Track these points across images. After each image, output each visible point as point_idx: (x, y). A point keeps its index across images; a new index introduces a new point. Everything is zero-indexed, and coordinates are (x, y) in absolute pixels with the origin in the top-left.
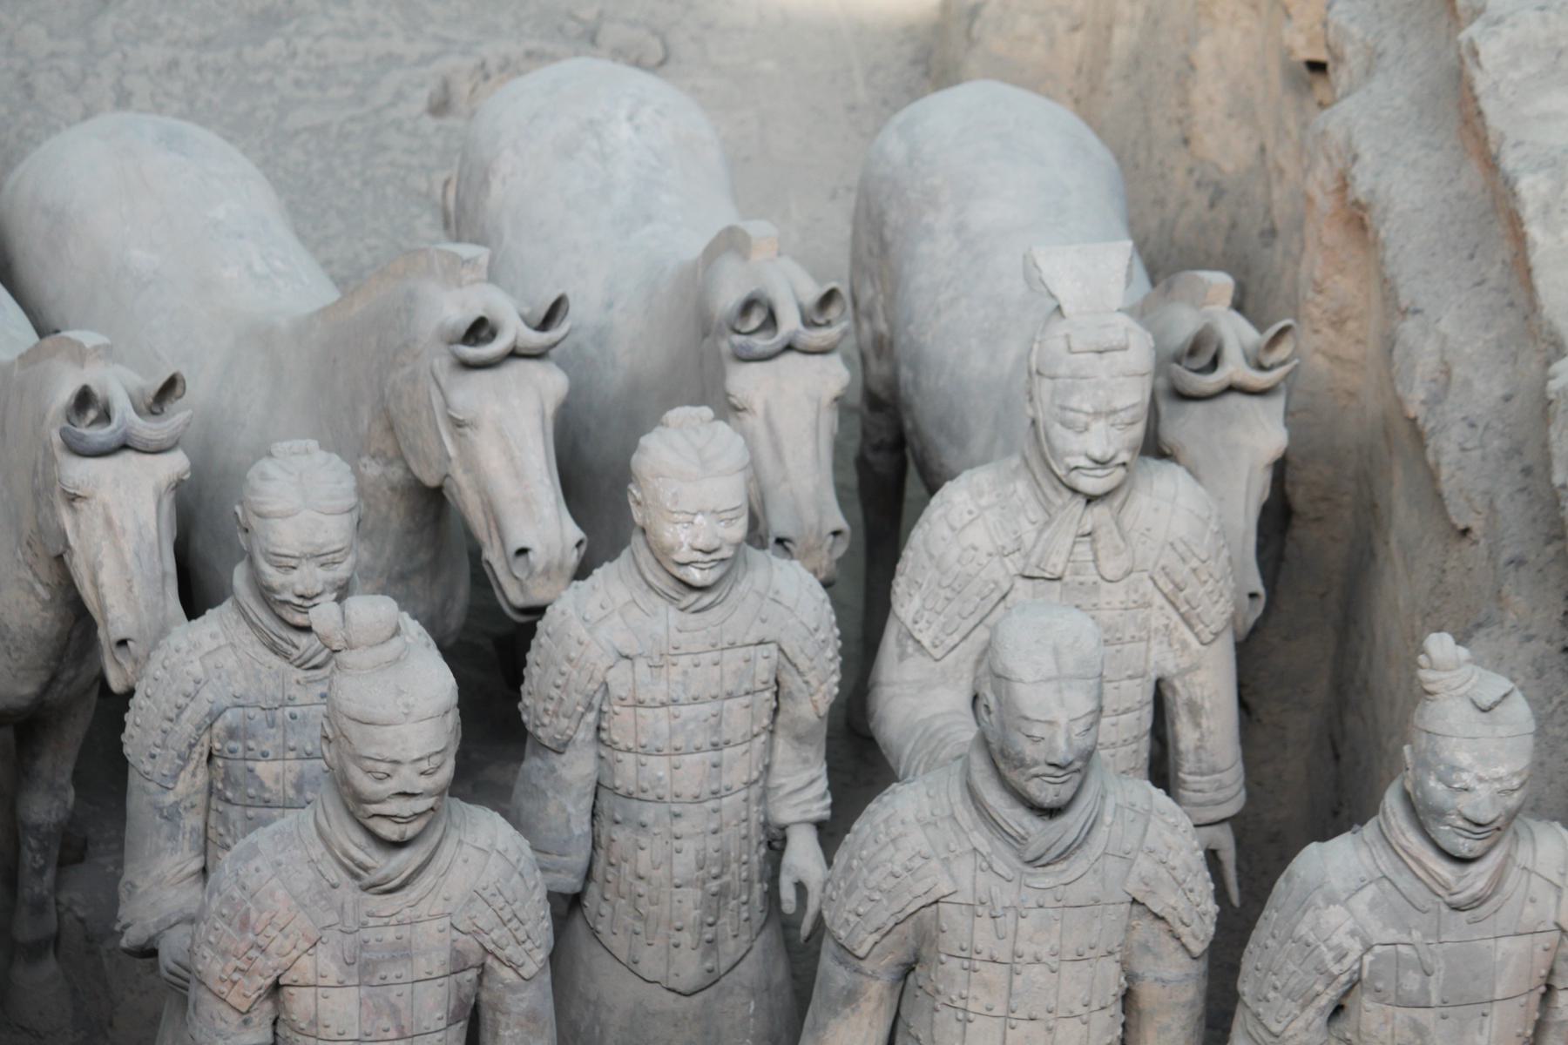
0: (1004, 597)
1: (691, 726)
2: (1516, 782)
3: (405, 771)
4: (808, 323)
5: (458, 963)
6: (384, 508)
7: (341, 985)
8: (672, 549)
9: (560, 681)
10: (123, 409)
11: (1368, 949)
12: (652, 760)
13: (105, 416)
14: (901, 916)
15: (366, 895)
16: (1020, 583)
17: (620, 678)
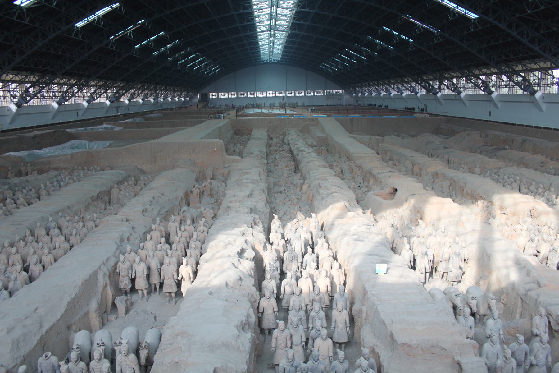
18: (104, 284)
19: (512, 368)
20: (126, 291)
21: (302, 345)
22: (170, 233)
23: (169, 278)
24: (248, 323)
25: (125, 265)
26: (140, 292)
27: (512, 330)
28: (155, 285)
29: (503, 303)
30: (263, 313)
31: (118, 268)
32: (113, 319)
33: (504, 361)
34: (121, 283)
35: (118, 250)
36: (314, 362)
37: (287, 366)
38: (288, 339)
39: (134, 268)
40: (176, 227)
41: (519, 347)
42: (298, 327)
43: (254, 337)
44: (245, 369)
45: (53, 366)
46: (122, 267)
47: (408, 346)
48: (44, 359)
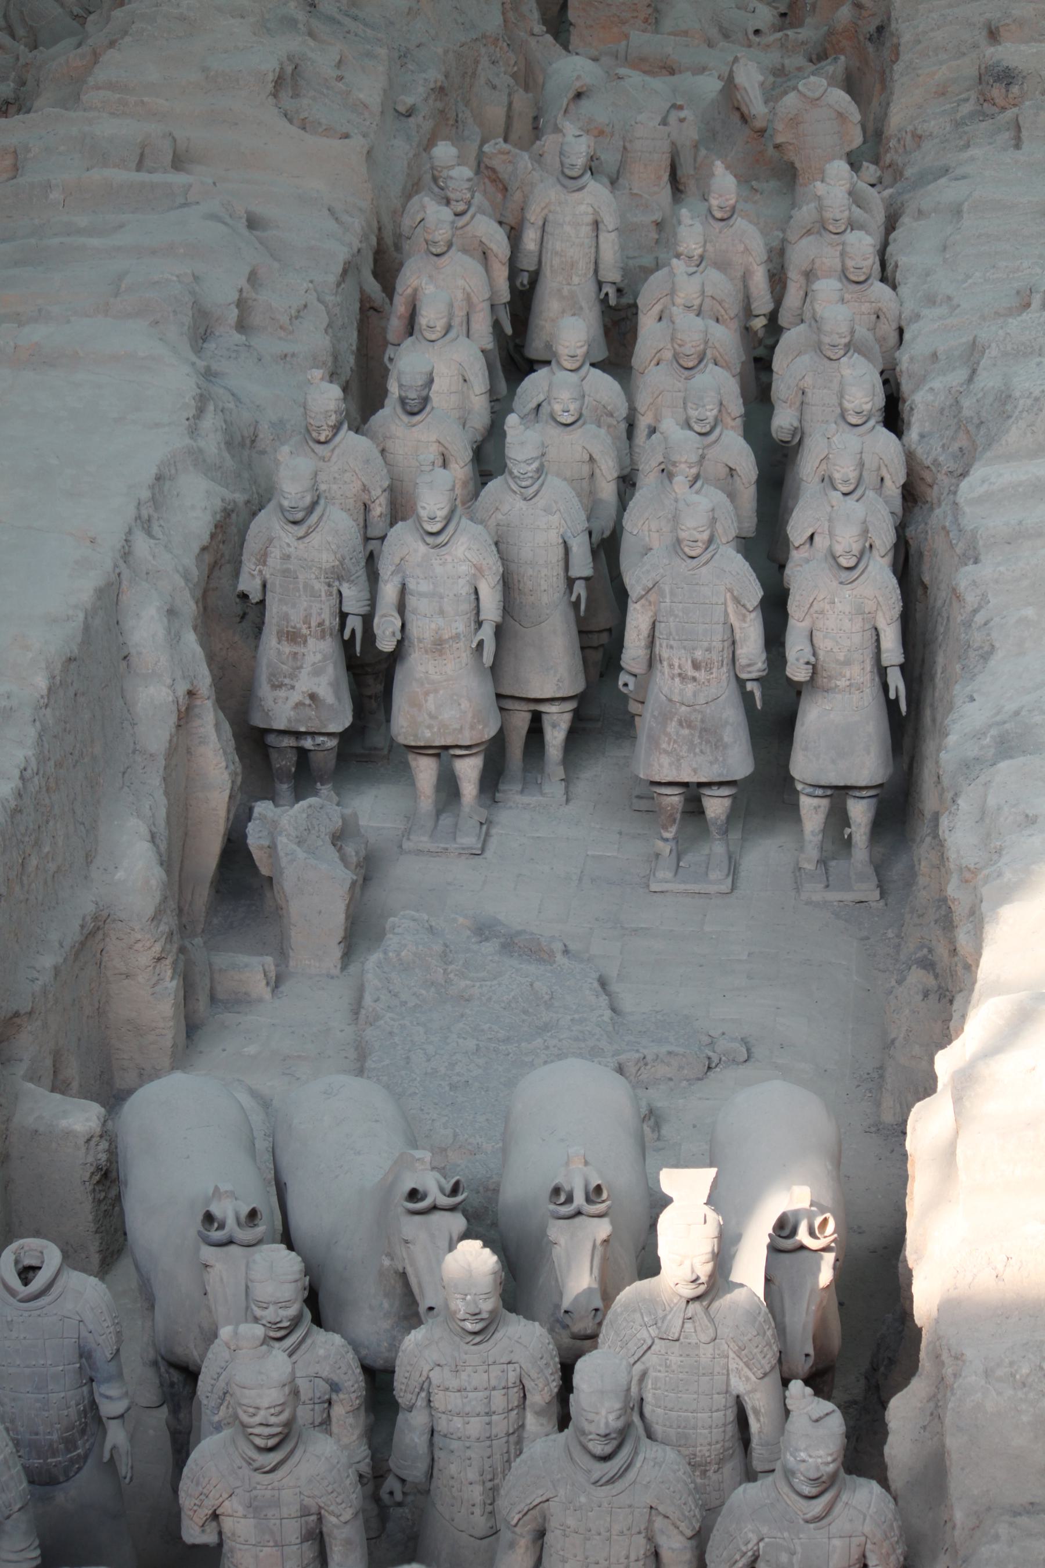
0: (650, 1348)
1: (474, 1403)
2: (830, 1459)
3: (262, 1413)
4: (588, 1200)
5: (305, 1512)
6: (393, 1282)
7: (245, 1517)
8: (455, 1312)
9: (407, 1375)
10: (231, 1222)
11: (762, 1539)
12: (455, 1418)
13: (221, 1226)
14: (531, 1506)
15: (256, 1474)
16: (657, 1341)
17: (436, 1376)
18: (182, 689)
20: (303, 754)
22: (535, 277)
23: (696, 666)
25: (316, 539)
26: (426, 770)
28: (537, 718)
31: (249, 565)
32: (259, 987)
34: (276, 687)
35: (211, 408)
39: (399, 568)
40: (596, 224)
45: (85, 1354)
46: (287, 557)
48: (12, 1292)
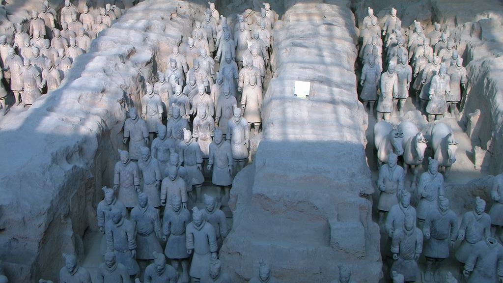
19: (416, 242)
21: (155, 185)
23: (29, 85)
24: (81, 150)
27: (477, 190)
29: (490, 152)
30: (129, 138)
33: (404, 231)
36: (141, 208)
37: (105, 209)
38: (134, 176)
41: (442, 214)
42: (149, 161)
43: (82, 169)
44: (45, 209)
47: (266, 199)
